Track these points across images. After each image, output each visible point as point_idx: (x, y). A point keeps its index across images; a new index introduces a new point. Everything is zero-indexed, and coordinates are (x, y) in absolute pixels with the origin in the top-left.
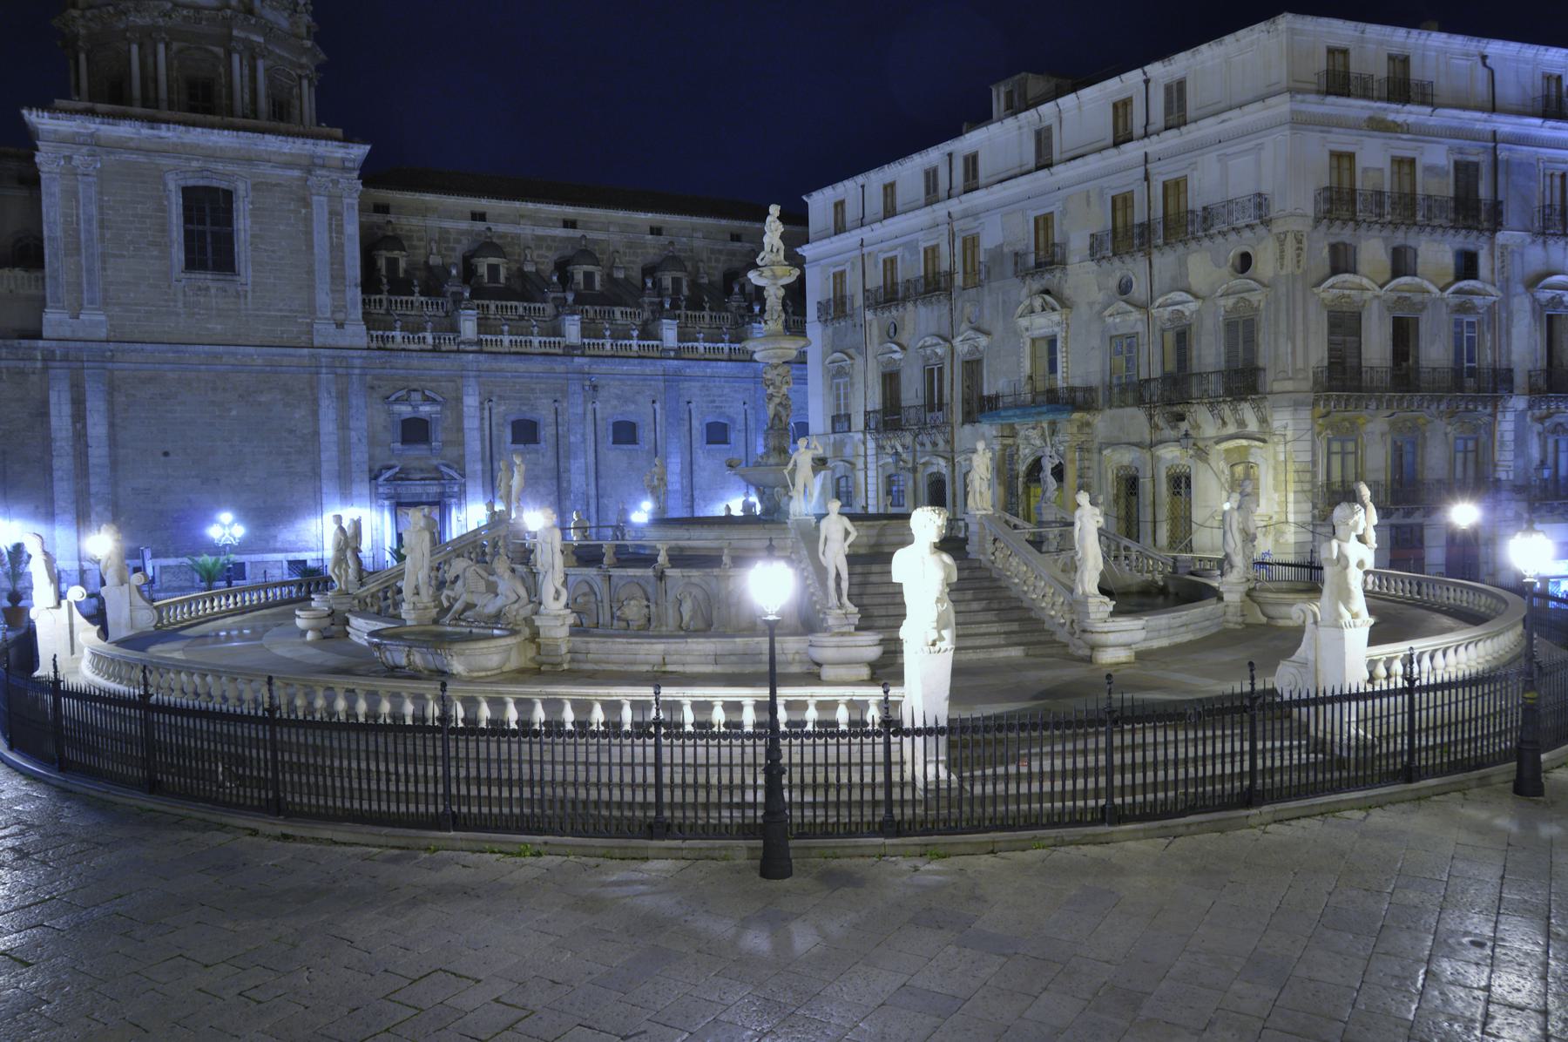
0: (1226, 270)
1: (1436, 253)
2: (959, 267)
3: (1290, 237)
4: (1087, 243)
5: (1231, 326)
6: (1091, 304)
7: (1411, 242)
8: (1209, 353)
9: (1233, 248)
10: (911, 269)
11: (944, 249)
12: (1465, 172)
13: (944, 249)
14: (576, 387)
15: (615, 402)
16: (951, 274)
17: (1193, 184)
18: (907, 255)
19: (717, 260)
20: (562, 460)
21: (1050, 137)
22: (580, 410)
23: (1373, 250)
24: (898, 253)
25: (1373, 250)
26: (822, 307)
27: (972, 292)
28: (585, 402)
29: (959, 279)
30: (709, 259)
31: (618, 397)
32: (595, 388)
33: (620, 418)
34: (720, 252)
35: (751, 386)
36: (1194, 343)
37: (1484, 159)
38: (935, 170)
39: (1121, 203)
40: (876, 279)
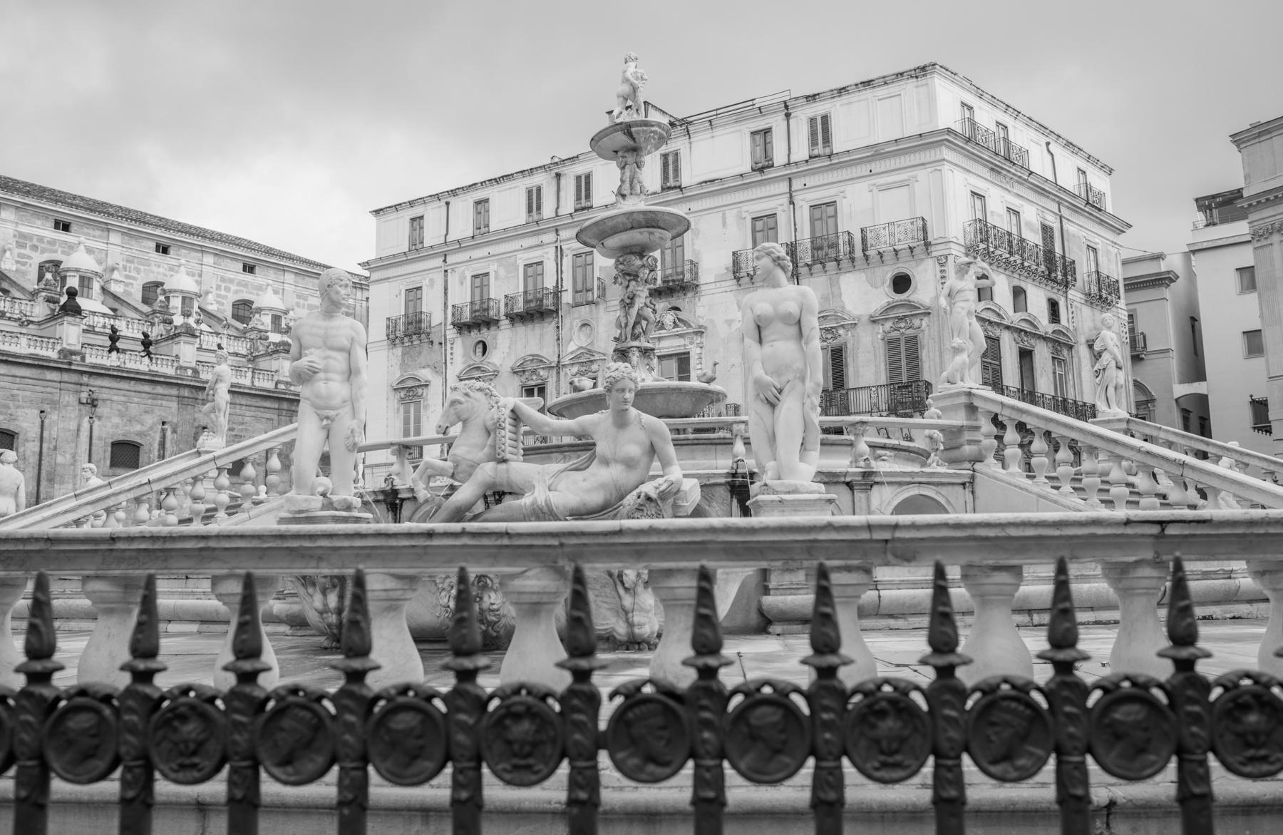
0: (887, 287)
1: (1037, 298)
2: (568, 284)
3: (951, 259)
4: (729, 261)
5: (891, 344)
6: (729, 322)
7: (1023, 285)
8: (868, 369)
9: (889, 273)
10: (506, 287)
11: (550, 267)
12: (1046, 230)
13: (550, 267)
14: (69, 398)
15: (116, 420)
16: (557, 294)
17: (843, 208)
18: (502, 272)
19: (227, 289)
20: (43, 483)
21: (676, 161)
22: (73, 425)
23: (1002, 286)
24: (492, 268)
25: (1002, 286)
26: (392, 324)
27: (584, 310)
28: (81, 417)
29: (567, 298)
30: (218, 287)
31: (121, 415)
32: (93, 403)
33: (121, 438)
34: (231, 281)
35: (275, 417)
36: (850, 360)
37: (1056, 226)
38: (539, 189)
39: (764, 226)
40: (461, 295)
